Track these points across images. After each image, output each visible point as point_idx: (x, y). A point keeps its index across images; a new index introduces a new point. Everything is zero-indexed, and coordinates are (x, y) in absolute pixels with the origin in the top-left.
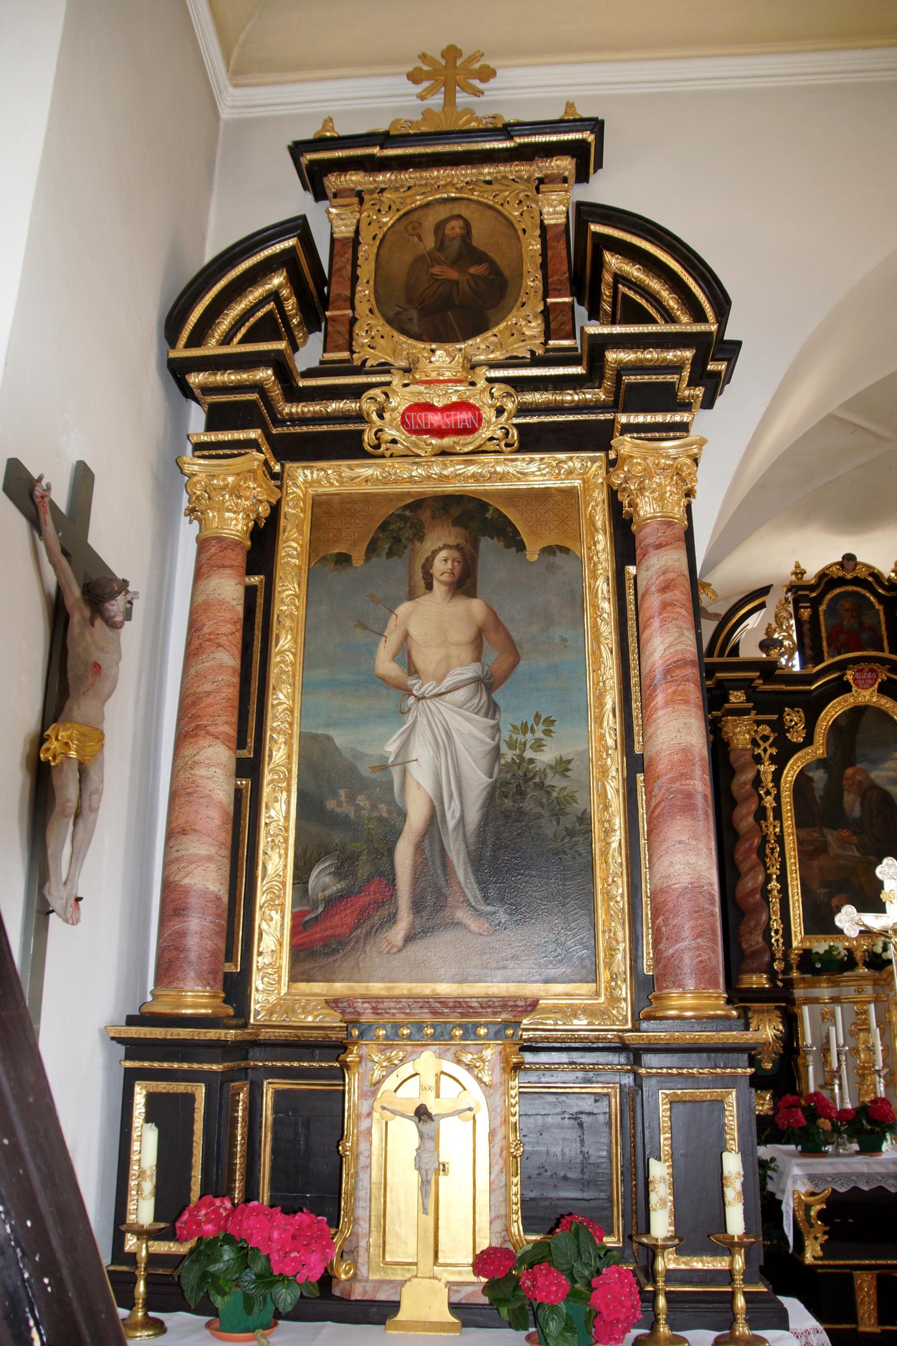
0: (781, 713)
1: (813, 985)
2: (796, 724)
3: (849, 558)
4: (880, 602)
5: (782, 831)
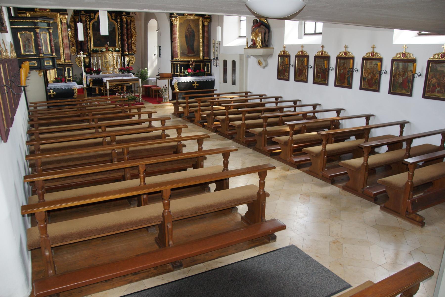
0: (90, 13)
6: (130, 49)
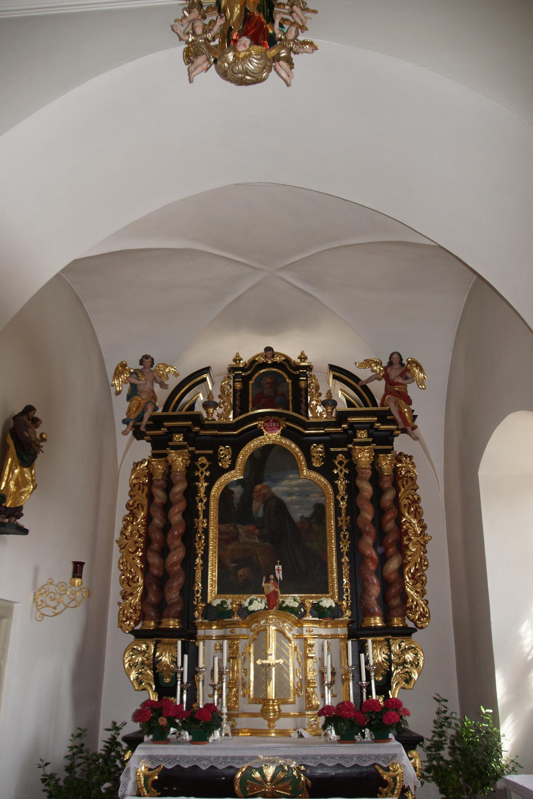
1: (210, 626)
2: (226, 456)
3: (268, 349)
4: (290, 379)
5: (208, 526)
6: (395, 602)
